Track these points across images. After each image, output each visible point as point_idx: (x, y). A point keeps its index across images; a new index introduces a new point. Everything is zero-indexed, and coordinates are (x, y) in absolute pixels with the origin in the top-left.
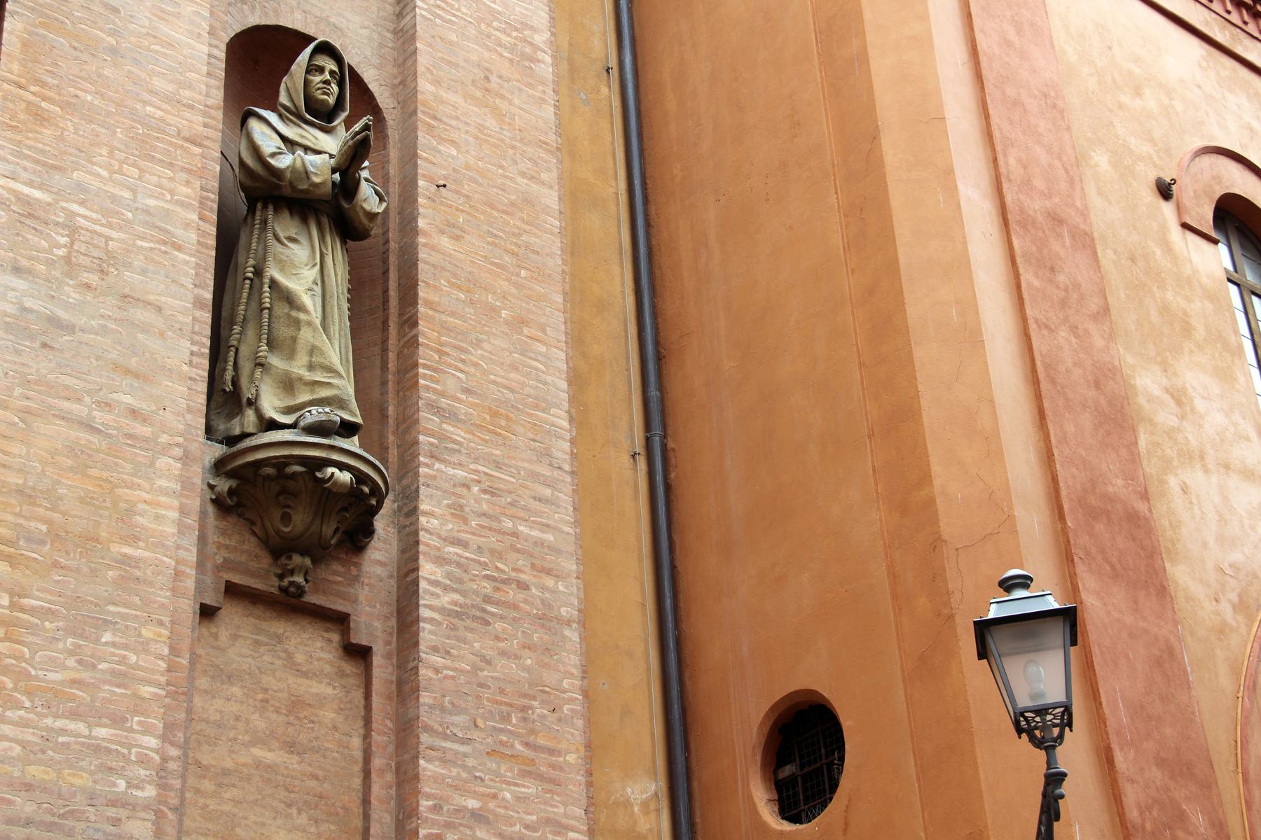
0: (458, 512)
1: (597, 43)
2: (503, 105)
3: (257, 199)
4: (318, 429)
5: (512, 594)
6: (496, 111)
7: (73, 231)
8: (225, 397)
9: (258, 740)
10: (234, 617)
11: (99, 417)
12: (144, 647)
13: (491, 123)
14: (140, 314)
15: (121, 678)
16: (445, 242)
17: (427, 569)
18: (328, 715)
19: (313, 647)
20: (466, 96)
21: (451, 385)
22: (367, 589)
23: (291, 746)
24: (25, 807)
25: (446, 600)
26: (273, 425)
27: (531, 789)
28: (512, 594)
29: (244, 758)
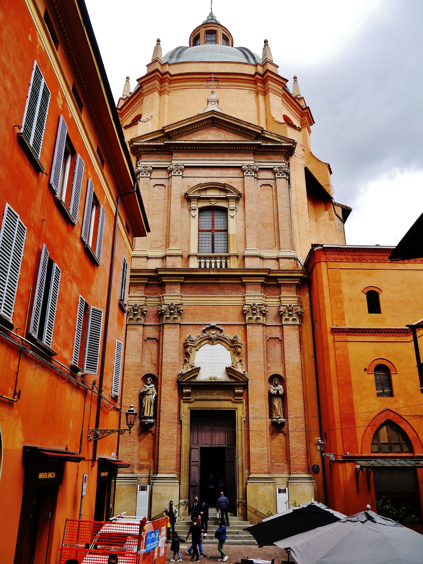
0: (292, 421)
1: (311, 353)
2: (295, 374)
3: (271, 397)
4: (277, 419)
5: (298, 427)
6: (295, 375)
7: (255, 408)
8: (271, 416)
9: (277, 443)
10: (274, 433)
11: (259, 424)
12: (265, 442)
13: (294, 377)
14: (262, 414)
15: (263, 444)
16: (290, 393)
17: (290, 427)
18: (283, 440)
19: (281, 435)
20: (292, 375)
21: (291, 408)
22: (285, 430)
23: (280, 443)
24: (258, 455)
25: (291, 429)
26: (274, 418)
27: (300, 444)
28: (298, 427)
29: (276, 445)
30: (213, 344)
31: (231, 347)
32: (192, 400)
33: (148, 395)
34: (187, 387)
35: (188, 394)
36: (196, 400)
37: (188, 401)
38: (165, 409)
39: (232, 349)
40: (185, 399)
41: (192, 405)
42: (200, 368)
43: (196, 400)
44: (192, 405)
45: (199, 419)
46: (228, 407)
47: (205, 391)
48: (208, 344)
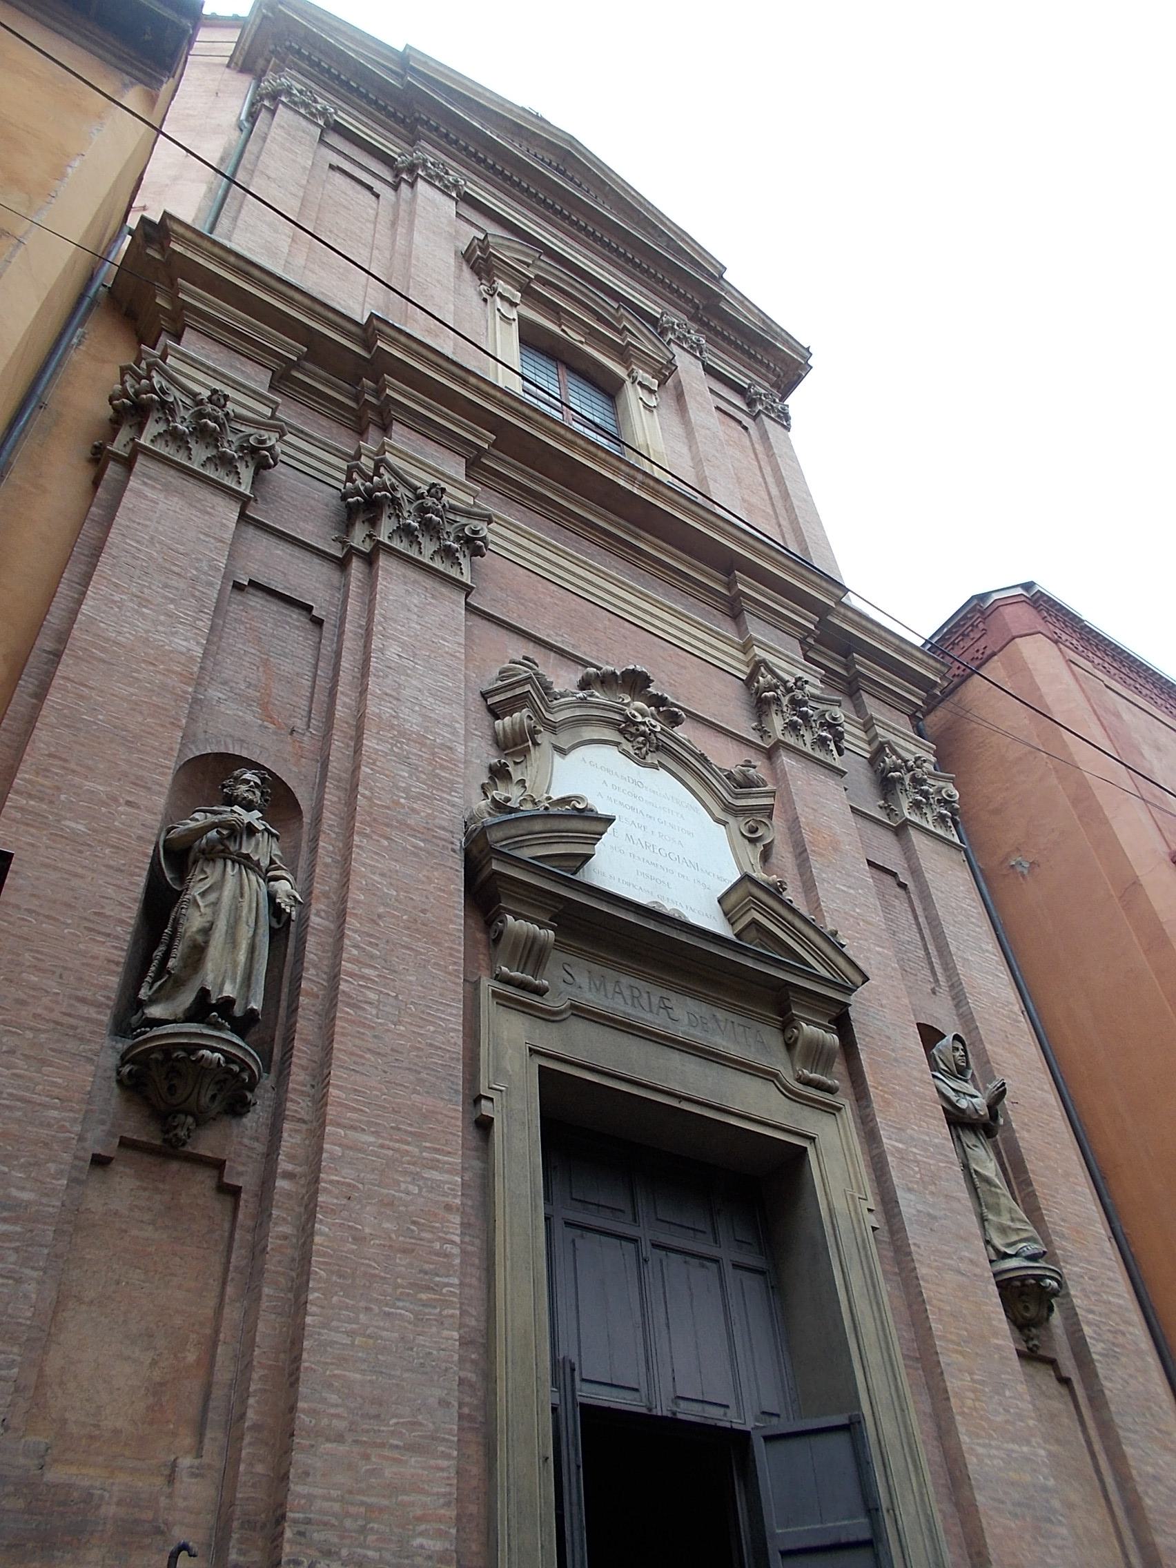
30: (641, 760)
31: (728, 808)
32: (552, 1002)
33: (246, 862)
34: (534, 899)
35: (533, 954)
36: (578, 1011)
37: (523, 998)
38: (372, 996)
39: (735, 823)
40: (508, 981)
41: (551, 1039)
42: (609, 820)
43: (578, 1011)
44: (551, 1039)
45: (606, 1148)
46: (765, 1116)
47: (626, 980)
48: (613, 752)
